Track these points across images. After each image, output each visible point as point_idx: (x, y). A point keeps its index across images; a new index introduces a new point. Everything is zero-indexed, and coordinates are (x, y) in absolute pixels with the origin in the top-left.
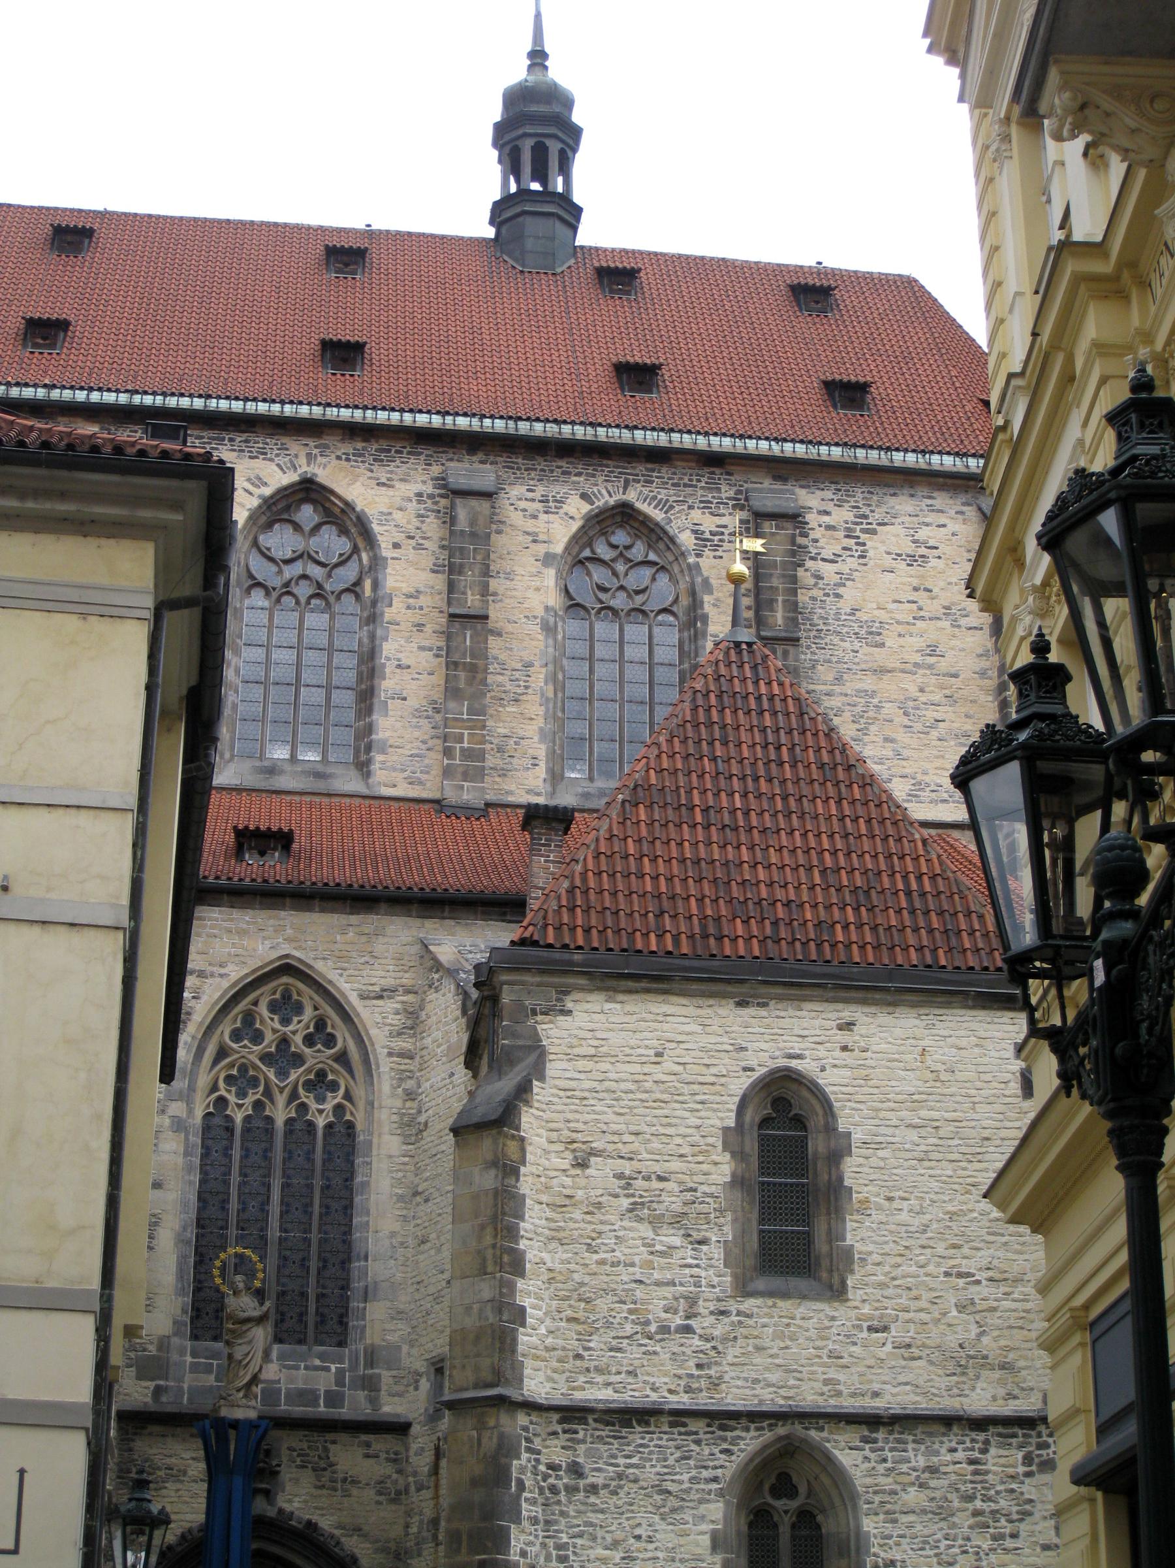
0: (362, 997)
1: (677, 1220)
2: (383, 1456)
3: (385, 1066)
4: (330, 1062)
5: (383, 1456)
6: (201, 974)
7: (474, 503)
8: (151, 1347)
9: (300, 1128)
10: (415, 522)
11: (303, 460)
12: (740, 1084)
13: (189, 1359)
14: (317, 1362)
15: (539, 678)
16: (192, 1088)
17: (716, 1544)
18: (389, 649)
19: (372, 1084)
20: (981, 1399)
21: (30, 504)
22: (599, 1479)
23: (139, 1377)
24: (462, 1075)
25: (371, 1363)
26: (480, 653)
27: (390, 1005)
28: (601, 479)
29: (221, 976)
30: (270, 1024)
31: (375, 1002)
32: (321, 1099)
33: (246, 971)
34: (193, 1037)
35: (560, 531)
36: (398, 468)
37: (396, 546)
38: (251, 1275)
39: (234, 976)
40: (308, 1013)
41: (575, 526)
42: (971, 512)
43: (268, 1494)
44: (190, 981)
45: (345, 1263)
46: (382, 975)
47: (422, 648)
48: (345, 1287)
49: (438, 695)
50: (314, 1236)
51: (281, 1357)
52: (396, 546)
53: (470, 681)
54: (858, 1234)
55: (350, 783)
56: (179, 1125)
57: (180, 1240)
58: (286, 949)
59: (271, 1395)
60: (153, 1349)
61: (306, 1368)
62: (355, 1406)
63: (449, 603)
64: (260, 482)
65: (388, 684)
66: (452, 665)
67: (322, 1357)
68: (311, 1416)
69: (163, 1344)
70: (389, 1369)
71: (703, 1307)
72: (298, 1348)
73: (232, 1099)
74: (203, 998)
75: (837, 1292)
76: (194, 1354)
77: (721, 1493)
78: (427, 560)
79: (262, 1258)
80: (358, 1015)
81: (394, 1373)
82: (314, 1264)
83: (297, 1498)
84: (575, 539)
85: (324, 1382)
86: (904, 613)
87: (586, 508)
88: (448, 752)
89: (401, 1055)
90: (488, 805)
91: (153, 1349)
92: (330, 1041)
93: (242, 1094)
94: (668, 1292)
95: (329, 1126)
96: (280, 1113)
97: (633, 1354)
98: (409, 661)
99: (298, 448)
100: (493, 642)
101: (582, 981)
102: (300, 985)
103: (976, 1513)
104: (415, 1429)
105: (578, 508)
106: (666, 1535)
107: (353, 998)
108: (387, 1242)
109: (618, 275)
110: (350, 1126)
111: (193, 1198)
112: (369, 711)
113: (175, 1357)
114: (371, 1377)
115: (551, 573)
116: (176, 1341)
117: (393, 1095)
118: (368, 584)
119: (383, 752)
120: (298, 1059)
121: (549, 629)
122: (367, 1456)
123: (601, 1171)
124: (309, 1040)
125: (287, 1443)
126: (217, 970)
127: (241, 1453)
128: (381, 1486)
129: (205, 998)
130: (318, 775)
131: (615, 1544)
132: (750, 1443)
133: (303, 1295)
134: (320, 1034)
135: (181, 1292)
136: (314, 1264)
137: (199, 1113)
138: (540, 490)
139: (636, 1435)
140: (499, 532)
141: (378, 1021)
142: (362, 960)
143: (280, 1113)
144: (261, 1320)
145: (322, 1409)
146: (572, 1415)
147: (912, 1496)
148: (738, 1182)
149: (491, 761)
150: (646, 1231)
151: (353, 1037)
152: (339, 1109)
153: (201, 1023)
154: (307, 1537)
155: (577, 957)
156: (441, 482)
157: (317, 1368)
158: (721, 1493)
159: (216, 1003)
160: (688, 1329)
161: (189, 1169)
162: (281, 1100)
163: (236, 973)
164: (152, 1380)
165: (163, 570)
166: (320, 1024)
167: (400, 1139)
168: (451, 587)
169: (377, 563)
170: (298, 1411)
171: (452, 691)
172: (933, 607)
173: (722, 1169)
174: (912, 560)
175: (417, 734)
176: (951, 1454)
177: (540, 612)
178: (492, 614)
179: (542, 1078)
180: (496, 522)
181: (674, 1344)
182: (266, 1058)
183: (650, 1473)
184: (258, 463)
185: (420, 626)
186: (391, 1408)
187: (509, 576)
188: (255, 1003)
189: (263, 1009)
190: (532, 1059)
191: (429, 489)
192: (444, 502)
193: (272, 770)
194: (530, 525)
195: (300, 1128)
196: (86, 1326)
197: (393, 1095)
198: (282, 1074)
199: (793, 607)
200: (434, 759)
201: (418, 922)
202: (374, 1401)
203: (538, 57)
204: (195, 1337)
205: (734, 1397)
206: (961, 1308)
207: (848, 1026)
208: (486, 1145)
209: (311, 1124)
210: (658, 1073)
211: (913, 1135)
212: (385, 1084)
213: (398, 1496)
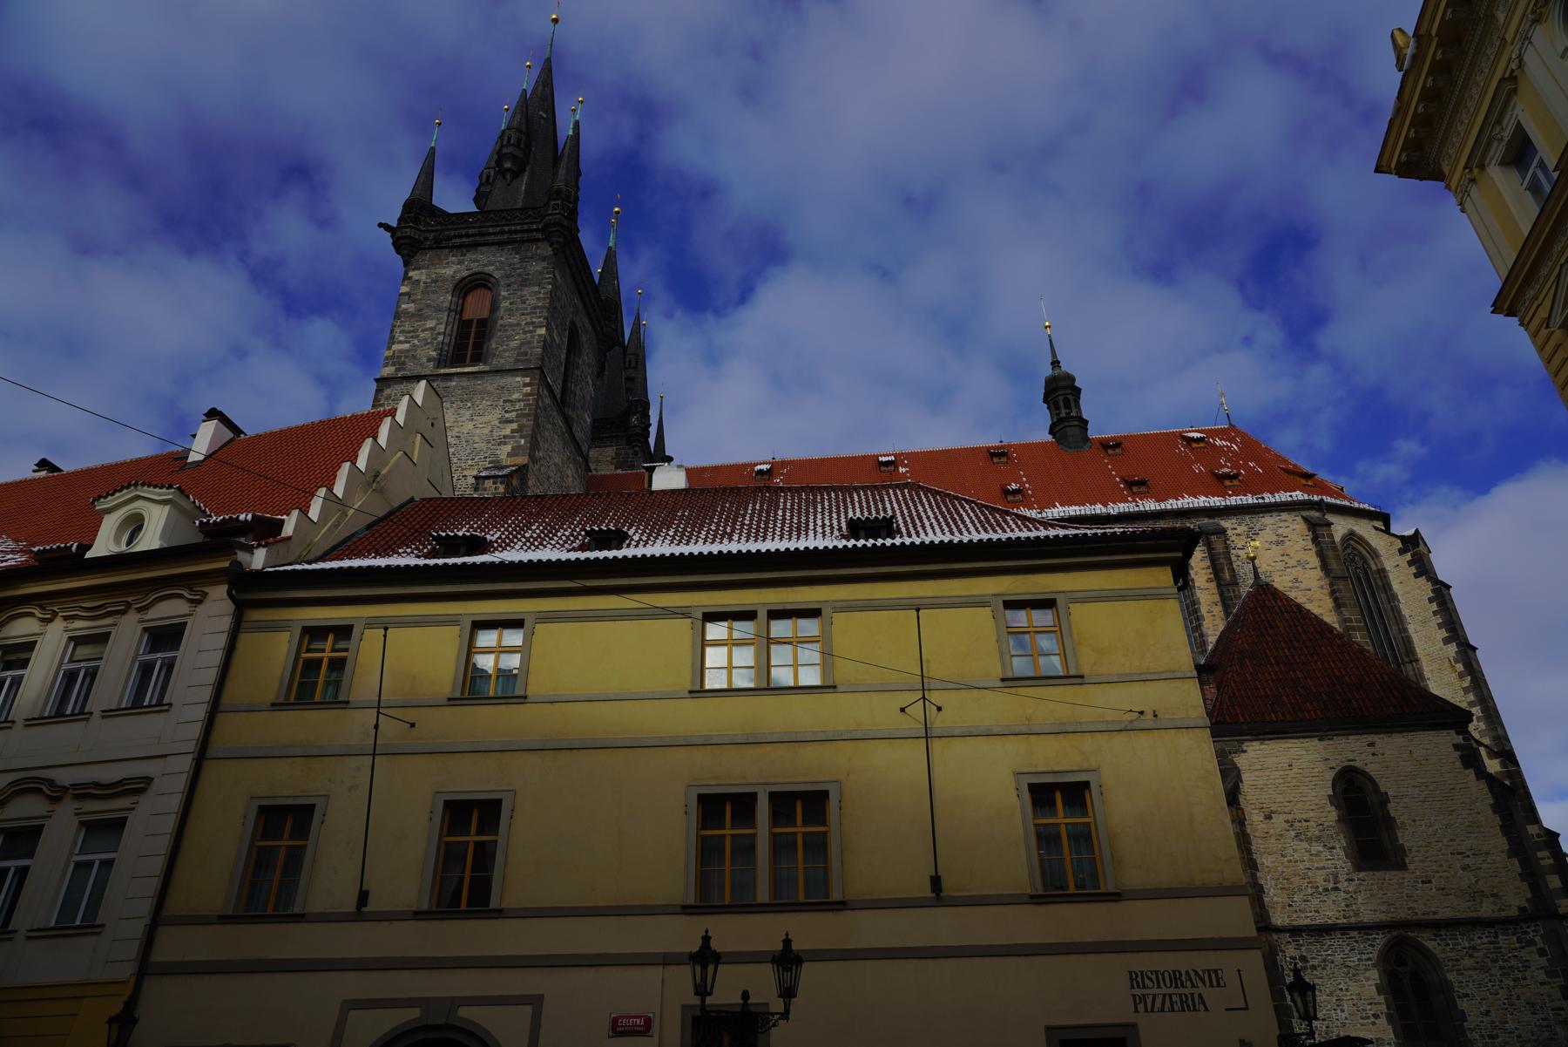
1: (1319, 839)
12: (1330, 776)
17: (1379, 989)
20: (1486, 910)
22: (1315, 962)
42: (1299, 519)
54: (1404, 838)
71: (1342, 878)
75: (1402, 866)
77: (1374, 966)
86: (1280, 566)
94: (1323, 872)
97: (1315, 902)
103: (1501, 968)
106: (1354, 988)
109: (1109, 446)
123: (1278, 821)
131: (1331, 994)
132: (1381, 939)
139: (1327, 941)
146: (1295, 931)
147: (1467, 962)
148: (1340, 820)
150: (1305, 845)
158: (1374, 966)
160: (1337, 889)
172: (1292, 562)
173: (1333, 815)
174: (1278, 543)
176: (1481, 939)
181: (1333, 895)
183: (1338, 958)
199: (1232, 570)
203: (1055, 363)
205: (1367, 916)
206: (1464, 869)
207: (1372, 744)
210: (1292, 774)
211: (1417, 791)
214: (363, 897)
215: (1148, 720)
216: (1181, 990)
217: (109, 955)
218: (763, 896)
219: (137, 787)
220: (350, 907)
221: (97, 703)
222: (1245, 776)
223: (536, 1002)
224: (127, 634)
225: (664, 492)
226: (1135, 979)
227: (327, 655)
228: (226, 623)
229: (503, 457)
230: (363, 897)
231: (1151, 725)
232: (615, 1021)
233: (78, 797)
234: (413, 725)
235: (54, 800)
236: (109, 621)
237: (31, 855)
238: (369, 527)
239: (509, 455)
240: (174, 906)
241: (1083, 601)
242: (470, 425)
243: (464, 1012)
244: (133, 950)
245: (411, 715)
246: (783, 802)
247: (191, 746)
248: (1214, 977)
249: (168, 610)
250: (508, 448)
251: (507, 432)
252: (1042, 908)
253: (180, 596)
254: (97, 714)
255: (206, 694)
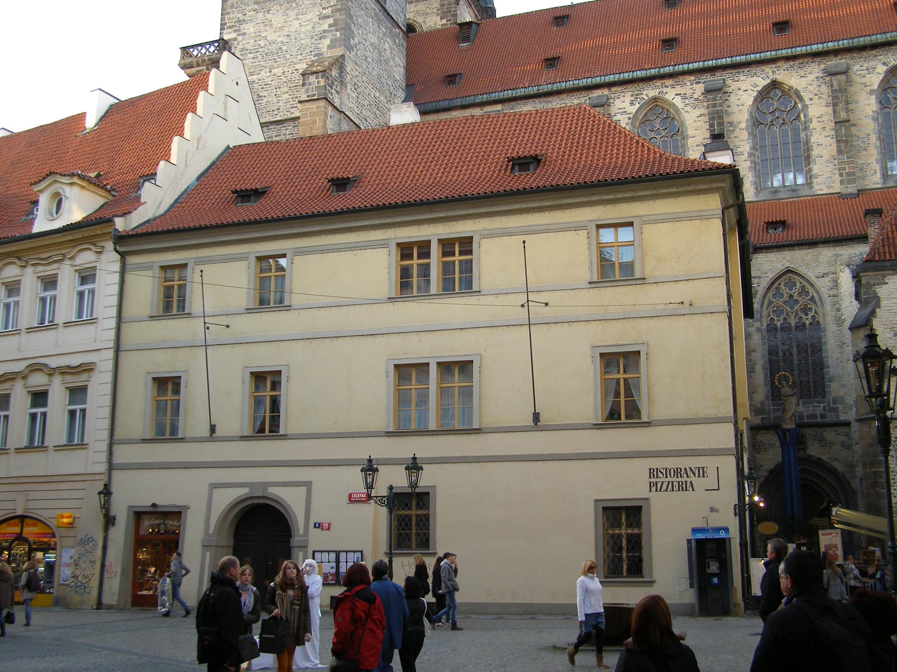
0: (817, 277)
3: (828, 301)
6: (759, 277)
7: (839, 77)
9: (801, 327)
10: (817, 89)
11: (771, 74)
15: (873, 139)
16: (761, 317)
18: (813, 139)
21: (680, 189)
24: (855, 303)
25: (834, 403)
26: (849, 135)
27: (827, 279)
28: (890, 55)
30: (785, 291)
32: (806, 314)
35: (875, 80)
36: (808, 69)
37: (811, 99)
38: (788, 381)
40: (798, 285)
41: (881, 77)
43: (804, 450)
44: (754, 281)
45: (822, 369)
46: (822, 270)
47: (826, 137)
48: (823, 378)
49: (835, 153)
50: (810, 362)
51: (803, 404)
52: (811, 99)
53: (846, 146)
55: (805, 192)
56: (758, 330)
57: (764, 368)
58: (787, 264)
59: (801, 416)
60: (759, 405)
62: (831, 418)
63: (834, 117)
64: (756, 85)
65: (815, 153)
66: (838, 141)
69: (762, 403)
73: (775, 318)
74: (759, 285)
78: (824, 103)
79: (793, 375)
82: (810, 371)
83: (814, 450)
84: (882, 81)
85: (819, 411)
87: (885, 68)
88: (841, 175)
89: (833, 296)
90: (858, 191)
91: (759, 405)
93: (778, 316)
95: (811, 324)
96: (793, 321)
98: (822, 142)
99: (768, 69)
100: (853, 129)
101: (890, 272)
104: (853, 424)
105: (882, 69)
107: (813, 279)
110: (818, 323)
111: (767, 353)
112: (809, 164)
113: (767, 407)
115: (874, 97)
116: (766, 402)
118: (802, 116)
119: (816, 178)
120: (797, 301)
121: (875, 119)
124: (800, 294)
125: (809, 432)
127: (793, 440)
128: (843, 444)
130: (793, 190)
133: (809, 382)
134: (803, 291)
135: (766, 385)
136: (810, 371)
137: (765, 325)
138: (866, 65)
140: (850, 86)
141: (823, 285)
143: (793, 321)
144: (793, 395)
149: (858, 174)
152: (813, 317)
154: (819, 462)
155: (888, 264)
156: (825, 71)
161: (764, 344)
162: (792, 317)
163: (771, 275)
165: (724, 199)
166: (803, 287)
168: (834, 112)
169: (805, 107)
171: (840, 152)
175: (828, 169)
177: (871, 113)
178: (851, 118)
179: (879, 307)
180: (849, 82)
182: (785, 302)
184: (754, 78)
185: (824, 129)
186: (843, 417)
187: (857, 102)
189: (782, 286)
190: (874, 302)
191: (820, 75)
192: (827, 78)
193: (776, 191)
194: (863, 80)
195: (801, 327)
196: (731, 427)
198: (792, 307)
200: (837, 178)
201: (833, 249)
202: (837, 416)
208: (863, 333)
209: (804, 324)
212: (828, 308)
213: (849, 447)
214: (213, 429)
215: (686, 309)
216: (680, 479)
217: (92, 460)
218: (432, 426)
219: (87, 368)
220: (206, 432)
221: (60, 319)
222: (883, 303)
223: (308, 485)
224: (67, 276)
225: (398, 127)
226: (652, 473)
227: (176, 283)
228: (117, 267)
229: (325, 49)
230: (213, 429)
231: (686, 311)
232: (350, 495)
233: (62, 373)
234: (228, 326)
235: (50, 375)
236: (55, 266)
237: (45, 405)
238: (198, 179)
239: (330, 47)
240: (119, 434)
241: (655, 222)
242: (296, 24)
243: (272, 490)
244: (104, 457)
245: (224, 320)
246: (446, 367)
247: (111, 344)
248: (701, 472)
249: (86, 258)
250: (327, 42)
251: (326, 27)
252: (600, 432)
253: (89, 249)
254: (61, 325)
255: (114, 312)
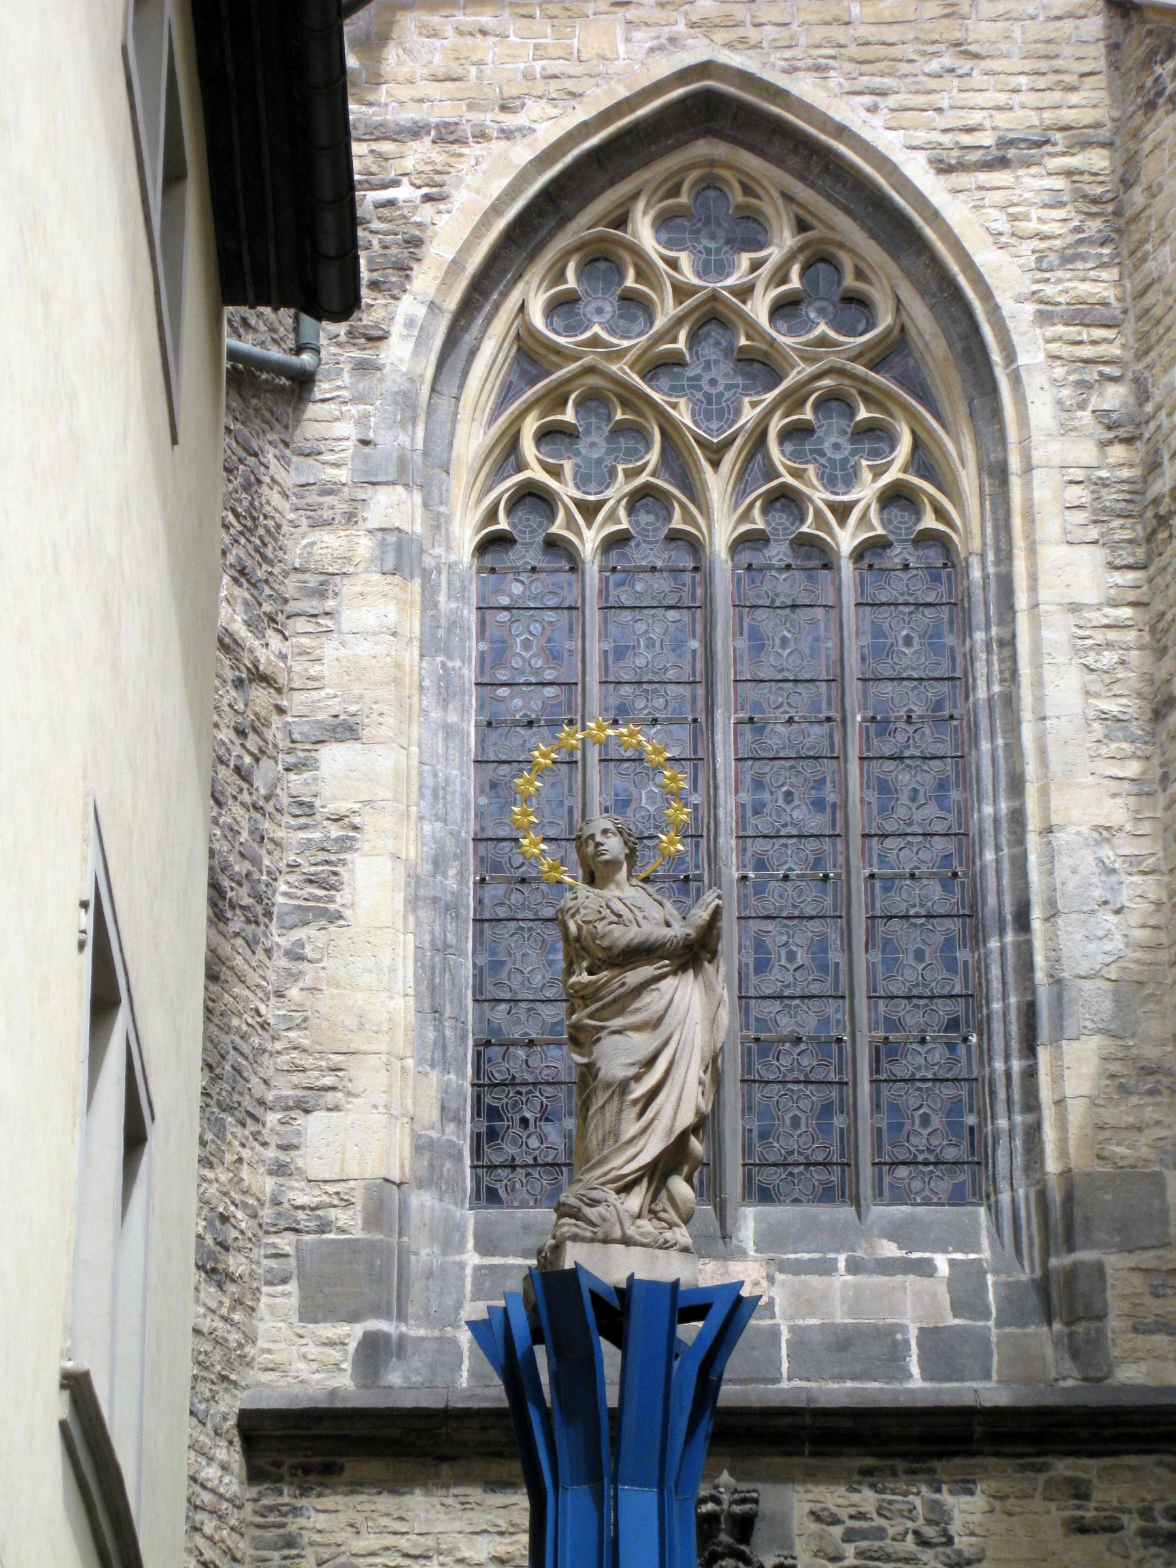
0: (943, 168)
2: (1132, 1523)
4: (859, 369)
5: (1132, 1523)
8: (341, 1217)
13: (472, 1259)
14: (890, 1250)
19: (996, 413)
23: (311, 1312)
27: (1032, 183)
29: (507, 134)
31: (983, 177)
33: (582, 114)
34: (433, 307)
39: (548, 133)
60: (350, 1222)
61: (854, 1267)
67: (895, 1233)
68: (886, 1402)
69: (384, 1202)
70: (1128, 1247)
72: (826, 1213)
76: (485, 1246)
80: (935, 217)
81: (1146, 1259)
91: (350, 1222)
92: (857, 305)
102: (751, 162)
108: (1087, 860)
113: (425, 1253)
114: (1071, 1274)
116: (423, 1201)
117: (1067, 430)
122: (1081, 1528)
126: (490, 118)
129: (460, 197)
142: (934, 65)
144: (693, 954)
145: (917, 1382)
151: (923, 291)
153: (456, 265)
157: (887, 1267)
159: (496, 209)
164: (354, 1317)
167: (1100, 555)
170: (836, 1390)
188: (621, 222)
189: (644, 232)
197: (1067, 430)
202: (1084, 1351)
204: (488, 1196)
